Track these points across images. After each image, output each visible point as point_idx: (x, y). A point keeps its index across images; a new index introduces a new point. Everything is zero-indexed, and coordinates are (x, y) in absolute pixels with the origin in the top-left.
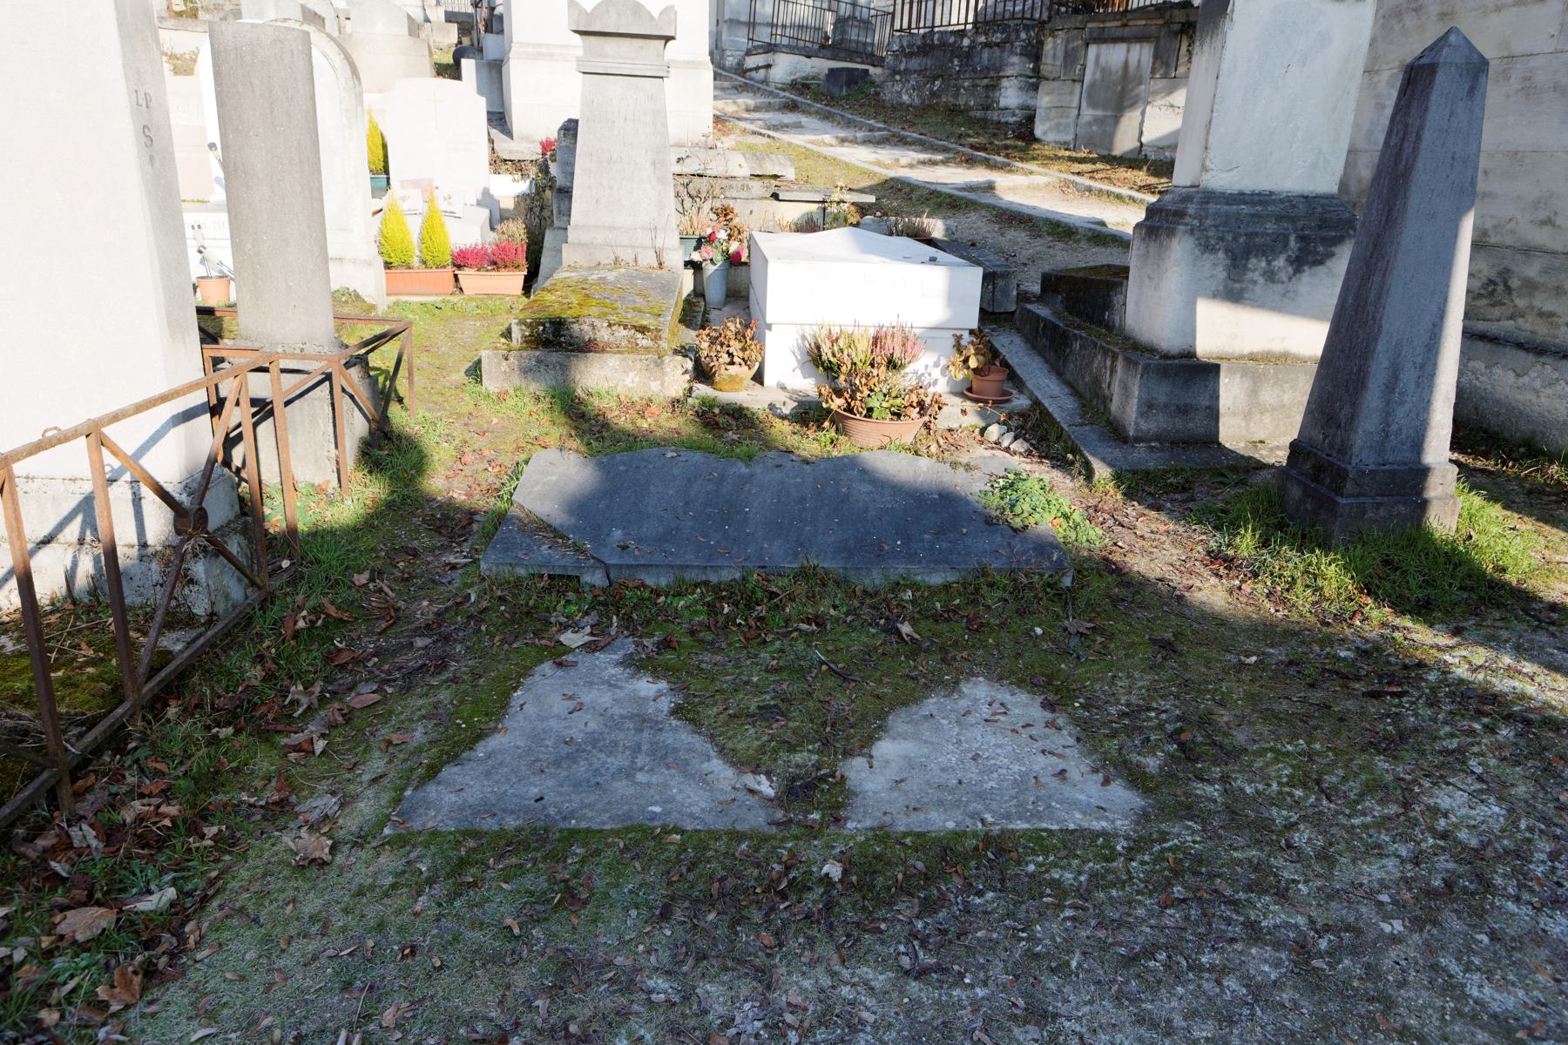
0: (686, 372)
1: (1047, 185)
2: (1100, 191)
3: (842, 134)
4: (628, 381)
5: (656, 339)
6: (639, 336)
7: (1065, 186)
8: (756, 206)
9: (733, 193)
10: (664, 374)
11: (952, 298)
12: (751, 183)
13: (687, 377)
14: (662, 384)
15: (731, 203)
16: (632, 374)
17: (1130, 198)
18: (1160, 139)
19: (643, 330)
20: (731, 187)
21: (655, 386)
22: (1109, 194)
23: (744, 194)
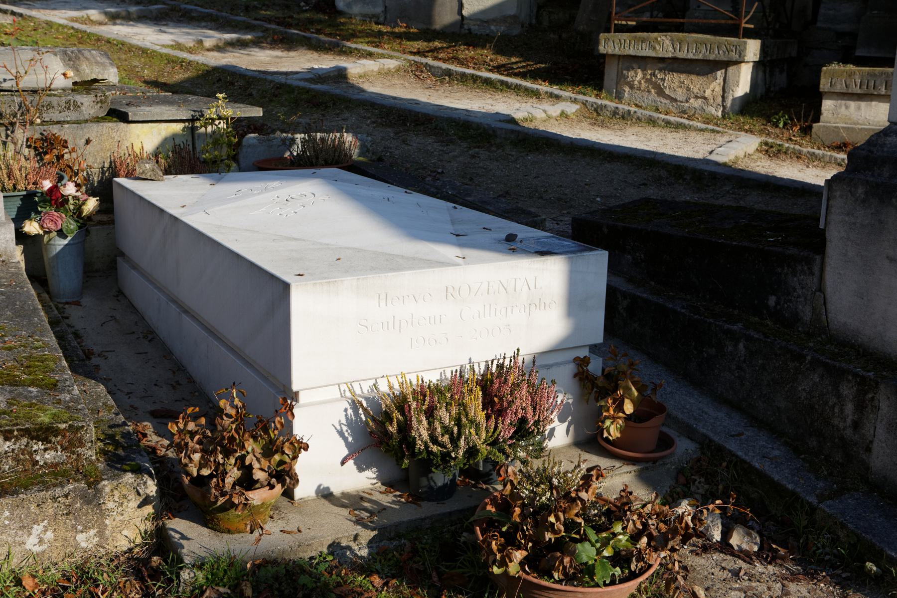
0: (146, 502)
1: (398, 70)
2: (463, 75)
3: (367, 40)
4: (31, 543)
5: (70, 447)
6: (39, 446)
7: (417, 71)
8: (93, 131)
9: (55, 115)
10: (103, 514)
11: (574, 304)
12: (79, 98)
13: (149, 509)
14: (101, 534)
15: (55, 130)
16: (37, 529)
17: (502, 83)
18: (484, 12)
19: (44, 434)
20: (50, 106)
21: (86, 540)
22: (475, 79)
23: (71, 116)
